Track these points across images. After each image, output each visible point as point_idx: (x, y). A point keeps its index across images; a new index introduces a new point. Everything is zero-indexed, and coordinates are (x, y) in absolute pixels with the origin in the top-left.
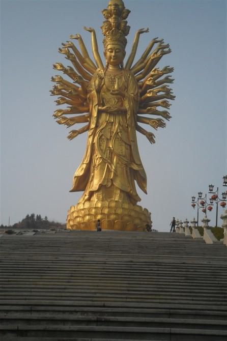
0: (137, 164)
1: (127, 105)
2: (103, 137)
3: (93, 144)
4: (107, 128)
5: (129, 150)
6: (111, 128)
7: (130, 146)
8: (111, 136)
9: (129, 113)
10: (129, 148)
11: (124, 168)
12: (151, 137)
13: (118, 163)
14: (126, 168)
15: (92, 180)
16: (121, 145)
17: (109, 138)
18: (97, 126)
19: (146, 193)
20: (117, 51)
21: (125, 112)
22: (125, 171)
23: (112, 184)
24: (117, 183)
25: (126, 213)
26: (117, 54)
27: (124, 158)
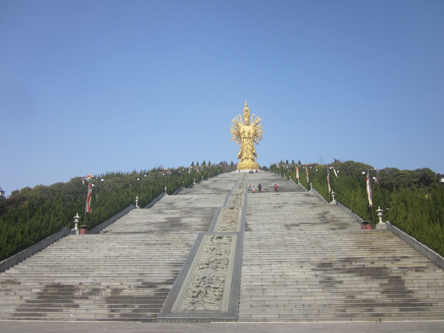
12: (258, 144)
21: (250, 137)
24: (250, 156)
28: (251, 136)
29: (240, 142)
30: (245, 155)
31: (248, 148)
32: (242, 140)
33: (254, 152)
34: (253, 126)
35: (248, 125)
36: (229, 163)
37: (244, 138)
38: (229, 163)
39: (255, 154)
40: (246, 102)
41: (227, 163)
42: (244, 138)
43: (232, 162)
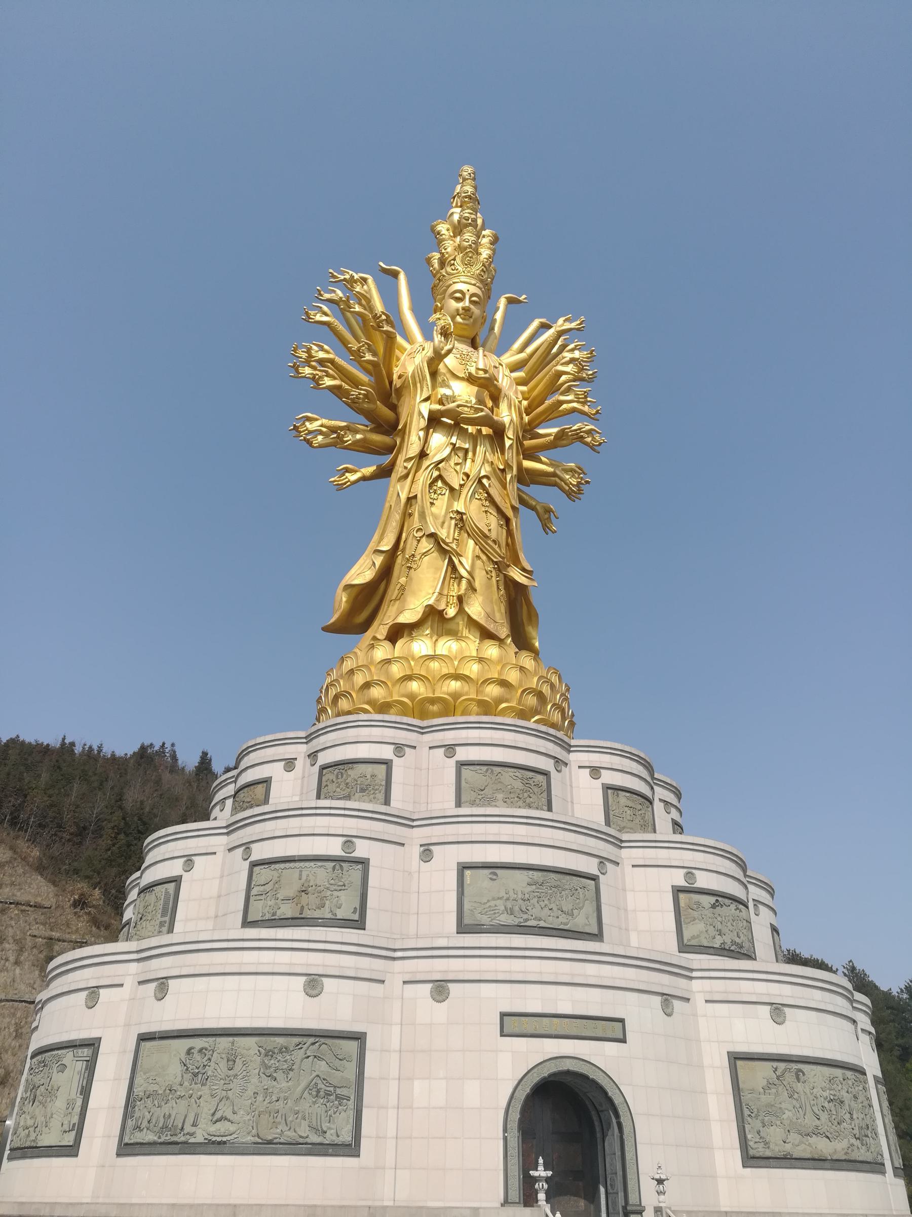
0: (524, 570)
1: (506, 415)
2: (440, 484)
3: (411, 500)
5: (504, 531)
7: (508, 521)
8: (461, 486)
9: (510, 433)
11: (494, 574)
13: (478, 557)
14: (498, 576)
16: (486, 512)
17: (457, 487)
18: (423, 455)
20: (474, 299)
22: (494, 579)
23: (461, 611)
25: (534, 682)
26: (472, 307)
27: (496, 547)
29: (385, 472)
30: (423, 587)
31: (461, 520)
36: (189, 760)
37: (434, 421)
38: (189, 760)
40: (467, 170)
41: (174, 757)
43: (205, 754)
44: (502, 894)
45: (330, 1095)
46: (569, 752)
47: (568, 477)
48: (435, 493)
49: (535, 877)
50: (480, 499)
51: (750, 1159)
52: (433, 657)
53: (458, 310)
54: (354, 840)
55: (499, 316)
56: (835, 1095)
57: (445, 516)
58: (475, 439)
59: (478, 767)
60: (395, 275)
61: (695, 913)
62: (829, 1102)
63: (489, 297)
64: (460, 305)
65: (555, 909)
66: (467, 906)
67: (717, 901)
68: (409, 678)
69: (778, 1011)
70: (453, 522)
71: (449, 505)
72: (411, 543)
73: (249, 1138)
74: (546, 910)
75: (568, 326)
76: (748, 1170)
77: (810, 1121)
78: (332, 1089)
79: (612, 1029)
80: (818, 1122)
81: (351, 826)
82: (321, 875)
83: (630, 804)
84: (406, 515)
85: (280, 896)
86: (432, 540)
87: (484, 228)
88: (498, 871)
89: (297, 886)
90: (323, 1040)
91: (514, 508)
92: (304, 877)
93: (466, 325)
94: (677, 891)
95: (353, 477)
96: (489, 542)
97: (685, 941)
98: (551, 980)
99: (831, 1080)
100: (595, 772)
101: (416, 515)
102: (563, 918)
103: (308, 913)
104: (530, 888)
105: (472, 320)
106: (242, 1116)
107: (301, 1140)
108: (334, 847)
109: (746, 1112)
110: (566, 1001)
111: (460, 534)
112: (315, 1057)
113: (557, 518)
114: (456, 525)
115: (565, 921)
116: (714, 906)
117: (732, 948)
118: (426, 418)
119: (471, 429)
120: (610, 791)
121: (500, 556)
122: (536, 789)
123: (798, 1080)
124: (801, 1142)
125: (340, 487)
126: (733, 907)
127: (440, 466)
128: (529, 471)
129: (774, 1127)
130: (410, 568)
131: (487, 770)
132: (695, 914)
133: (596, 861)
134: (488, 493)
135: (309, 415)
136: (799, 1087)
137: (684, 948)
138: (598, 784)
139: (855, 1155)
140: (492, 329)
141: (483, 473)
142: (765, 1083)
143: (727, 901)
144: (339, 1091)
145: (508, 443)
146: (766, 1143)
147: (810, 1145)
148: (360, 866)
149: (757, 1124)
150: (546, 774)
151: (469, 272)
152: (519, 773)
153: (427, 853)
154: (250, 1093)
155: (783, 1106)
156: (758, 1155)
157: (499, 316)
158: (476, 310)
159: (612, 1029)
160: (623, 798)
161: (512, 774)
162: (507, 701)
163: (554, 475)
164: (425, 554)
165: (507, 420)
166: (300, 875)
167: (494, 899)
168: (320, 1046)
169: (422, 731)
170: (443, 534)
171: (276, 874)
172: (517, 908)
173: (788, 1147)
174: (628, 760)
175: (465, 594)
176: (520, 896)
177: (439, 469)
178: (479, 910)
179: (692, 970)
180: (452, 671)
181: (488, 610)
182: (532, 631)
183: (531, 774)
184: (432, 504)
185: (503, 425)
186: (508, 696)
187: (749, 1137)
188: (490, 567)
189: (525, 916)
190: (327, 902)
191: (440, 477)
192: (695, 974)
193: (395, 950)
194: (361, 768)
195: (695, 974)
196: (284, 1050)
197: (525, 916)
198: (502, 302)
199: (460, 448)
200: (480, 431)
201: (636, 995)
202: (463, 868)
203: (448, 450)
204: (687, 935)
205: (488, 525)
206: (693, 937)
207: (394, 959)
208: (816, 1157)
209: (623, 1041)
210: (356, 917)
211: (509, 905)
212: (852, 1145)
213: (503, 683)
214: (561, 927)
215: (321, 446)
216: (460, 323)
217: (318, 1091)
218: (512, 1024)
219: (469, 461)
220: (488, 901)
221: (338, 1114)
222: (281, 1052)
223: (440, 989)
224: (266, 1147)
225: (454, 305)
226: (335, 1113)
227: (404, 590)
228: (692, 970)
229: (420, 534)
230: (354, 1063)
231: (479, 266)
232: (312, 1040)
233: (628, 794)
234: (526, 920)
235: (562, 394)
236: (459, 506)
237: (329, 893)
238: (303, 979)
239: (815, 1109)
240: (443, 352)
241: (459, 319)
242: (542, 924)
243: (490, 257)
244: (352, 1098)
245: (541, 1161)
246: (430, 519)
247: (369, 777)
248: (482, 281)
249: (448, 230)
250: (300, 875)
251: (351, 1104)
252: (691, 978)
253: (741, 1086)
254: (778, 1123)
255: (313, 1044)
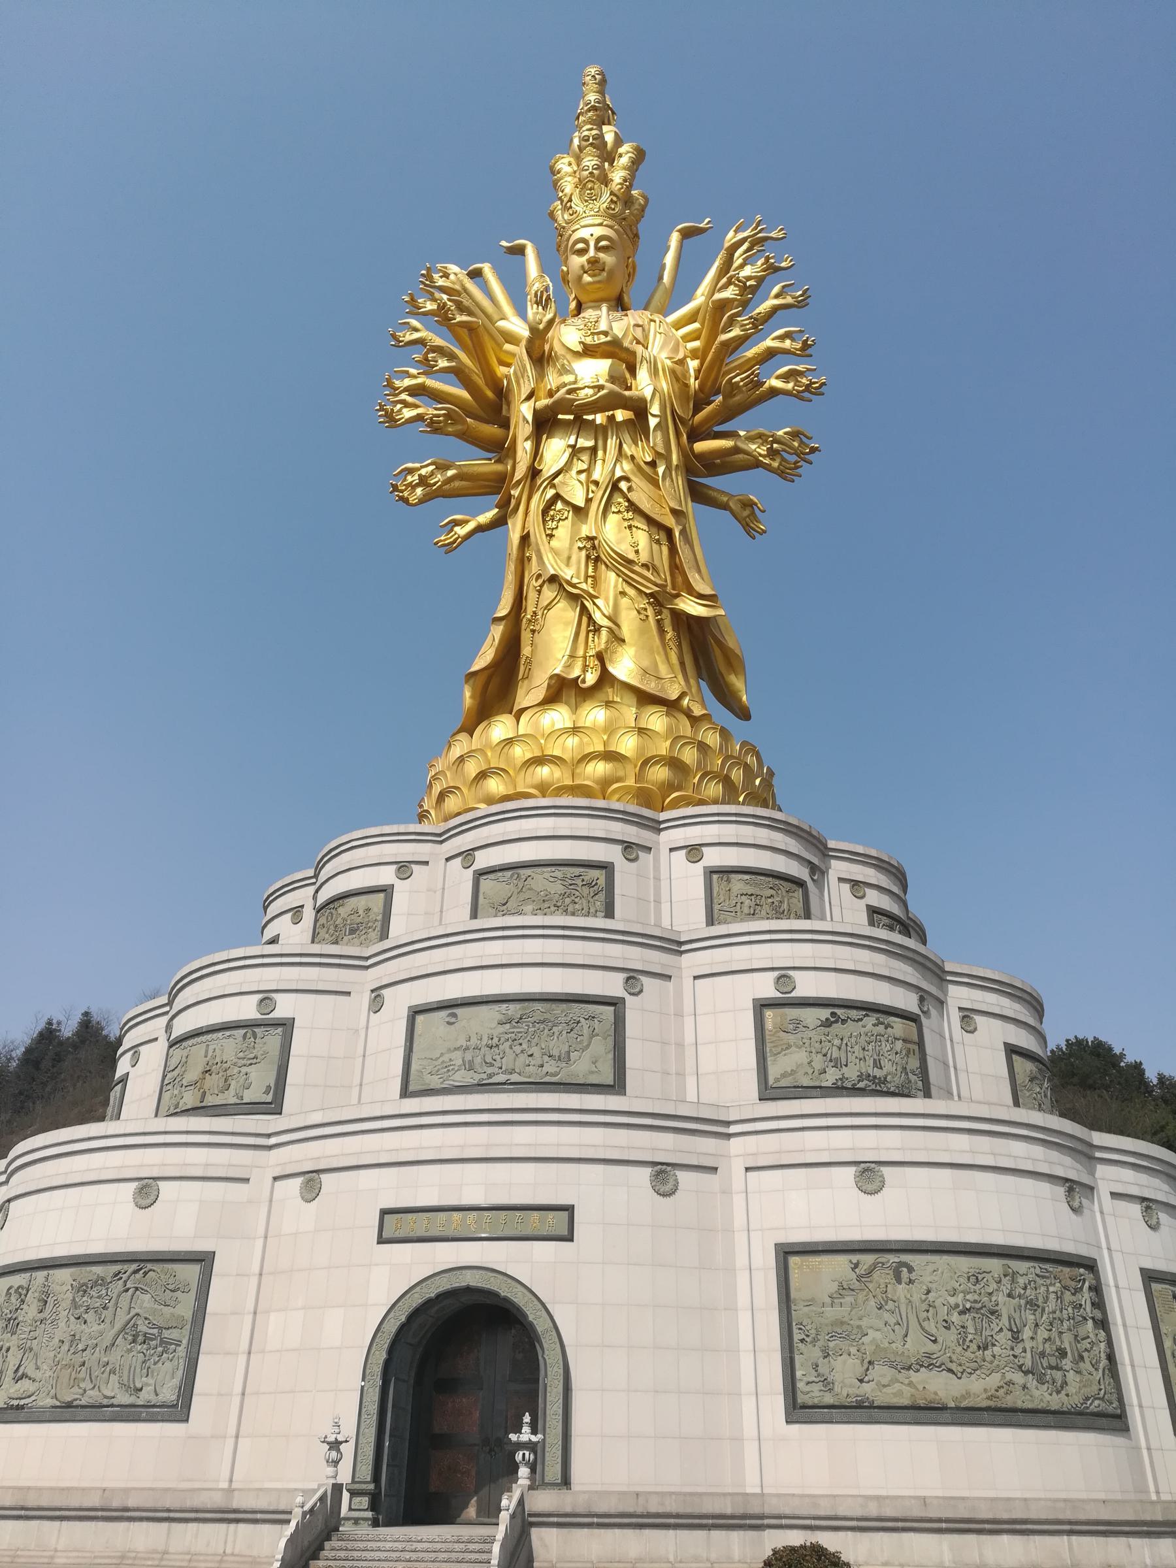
0: (701, 596)
1: (643, 384)
2: (559, 505)
3: (525, 539)
4: (573, 472)
5: (665, 550)
6: (588, 471)
7: (669, 532)
8: (589, 501)
9: (655, 409)
10: (663, 536)
11: (650, 612)
12: (747, 516)
13: (623, 593)
15: (526, 677)
16: (630, 527)
17: (581, 504)
19: (744, 714)
20: (603, 243)
24: (624, 667)
25: (663, 748)
26: (601, 255)
27: (648, 574)
28: (643, 384)
32: (524, 448)
33: (691, 607)
34: (678, 325)
35: (620, 304)
37: (545, 424)
39: (701, 647)
42: (545, 424)
44: (462, 1042)
45: (152, 1339)
46: (660, 830)
47: (753, 447)
48: (553, 520)
49: (510, 1012)
50: (619, 512)
51: (799, 1410)
52: (509, 742)
53: (583, 267)
54: (274, 995)
55: (669, 259)
56: (975, 1301)
57: (570, 548)
58: (600, 432)
59: (500, 874)
60: (520, 251)
61: (791, 1037)
62: (962, 1313)
63: (636, 236)
64: (583, 260)
65: (537, 1054)
66: (414, 1067)
67: (833, 1014)
68: (482, 775)
69: (869, 1174)
70: (584, 553)
71: (575, 530)
72: (532, 596)
73: (49, 1402)
74: (523, 1058)
75: (741, 236)
76: (796, 1427)
77: (917, 1345)
78: (155, 1331)
79: (557, 1222)
80: (932, 1347)
81: (268, 978)
82: (228, 1047)
83: (750, 890)
84: (523, 561)
85: (185, 1082)
86: (555, 586)
87: (619, 142)
88: (459, 1011)
89: (200, 1069)
90: (149, 1266)
91: (675, 513)
92: (210, 1053)
93: (599, 282)
94: (761, 1006)
95: (461, 531)
96: (637, 568)
97: (771, 1082)
98: (481, 1159)
99: (976, 1278)
100: (694, 852)
101: (534, 558)
102: (550, 1067)
103: (210, 1100)
104: (501, 1029)
105: (605, 274)
106: (46, 1372)
107: (105, 1402)
108: (247, 1009)
109: (797, 1336)
110: (475, 1186)
111: (595, 569)
112: (137, 1289)
113: (763, 512)
114: (588, 557)
115: (552, 1070)
116: (827, 1024)
117: (861, 1085)
118: (530, 420)
119: (600, 418)
120: (715, 877)
121: (656, 585)
122: (586, 890)
123: (899, 1281)
124: (894, 1381)
125: (450, 548)
126: (870, 1021)
127: (556, 481)
128: (700, 457)
129: (845, 1356)
130: (533, 631)
131: (512, 876)
132: (791, 1038)
133: (621, 977)
134: (628, 501)
135: (410, 465)
136: (901, 1291)
137: (768, 1092)
138: (698, 869)
139: (1017, 1399)
140: (661, 278)
141: (619, 473)
142: (834, 1287)
143: (854, 1014)
144: (166, 1333)
145: (653, 422)
146: (828, 1385)
147: (910, 1384)
148: (280, 1030)
149: (815, 1353)
150: (607, 867)
151: (592, 209)
152: (559, 873)
153: (377, 1000)
154: (56, 1340)
155: (864, 1323)
156: (810, 1404)
157: (669, 259)
158: (607, 259)
159: (557, 1222)
160: (738, 884)
161: (547, 875)
162: (618, 780)
163: (736, 450)
164: (548, 607)
165: (648, 393)
166: (207, 1051)
167: (449, 1051)
168: (146, 1274)
169: (440, 838)
170: (567, 573)
171: (185, 1052)
172: (478, 1060)
173: (867, 1389)
174: (751, 828)
175: (606, 649)
176: (485, 1041)
177: (554, 486)
178: (429, 1069)
179: (728, 1123)
180: (538, 753)
181: (646, 663)
182: (737, 682)
183: (577, 871)
184: (551, 536)
185: (643, 401)
186: (621, 773)
187: (799, 1374)
188: (643, 603)
189: (490, 1070)
190: (233, 1083)
191: (557, 497)
192: (733, 1129)
193: (269, 1136)
194: (353, 901)
195: (733, 1129)
196: (100, 1282)
197: (490, 1070)
198: (675, 237)
199: (583, 449)
200: (611, 419)
201: (600, 1168)
202: (416, 1012)
203: (567, 455)
204: (774, 1072)
205: (635, 545)
206: (784, 1075)
207: (270, 1148)
208: (922, 1403)
209: (570, 1238)
210: (269, 1098)
211: (468, 1056)
212: (1010, 1383)
213: (610, 756)
214: (547, 1079)
215: (422, 501)
216: (589, 283)
217: (135, 1337)
218: (396, 1225)
219: (599, 463)
220: (442, 1054)
221: (160, 1364)
222: (96, 1284)
223: (311, 1182)
224: (68, 1412)
225: (577, 261)
226: (155, 1363)
227: (530, 663)
228: (728, 1123)
229: (540, 581)
230: (193, 1294)
231: (606, 197)
232: (134, 1266)
233: (746, 877)
234: (490, 1076)
235: (724, 331)
236: (586, 530)
237: (236, 1070)
238: (133, 1185)
239: (931, 1327)
240: (541, 327)
241: (587, 278)
242: (515, 1078)
243: (625, 181)
244: (185, 1342)
245: (527, 1418)
246: (548, 558)
247: (361, 912)
248: (612, 217)
249: (570, 164)
250: (207, 1051)
251: (181, 1351)
252: (729, 1136)
253: (793, 1294)
254: (853, 1350)
255: (136, 1272)
